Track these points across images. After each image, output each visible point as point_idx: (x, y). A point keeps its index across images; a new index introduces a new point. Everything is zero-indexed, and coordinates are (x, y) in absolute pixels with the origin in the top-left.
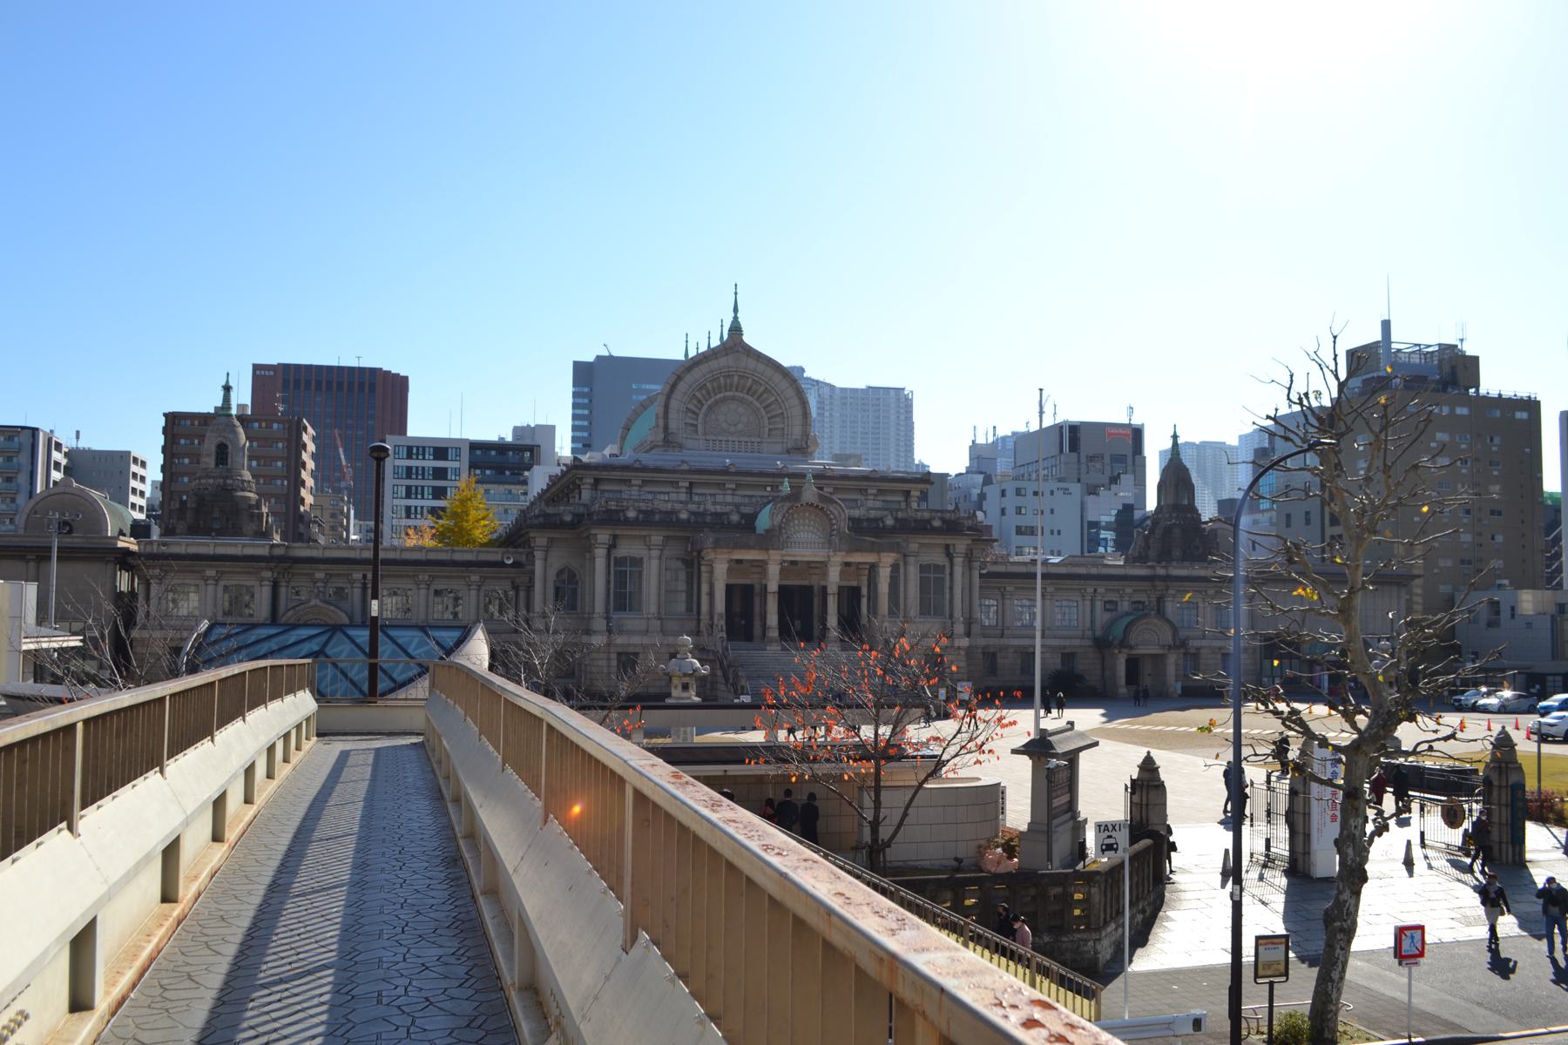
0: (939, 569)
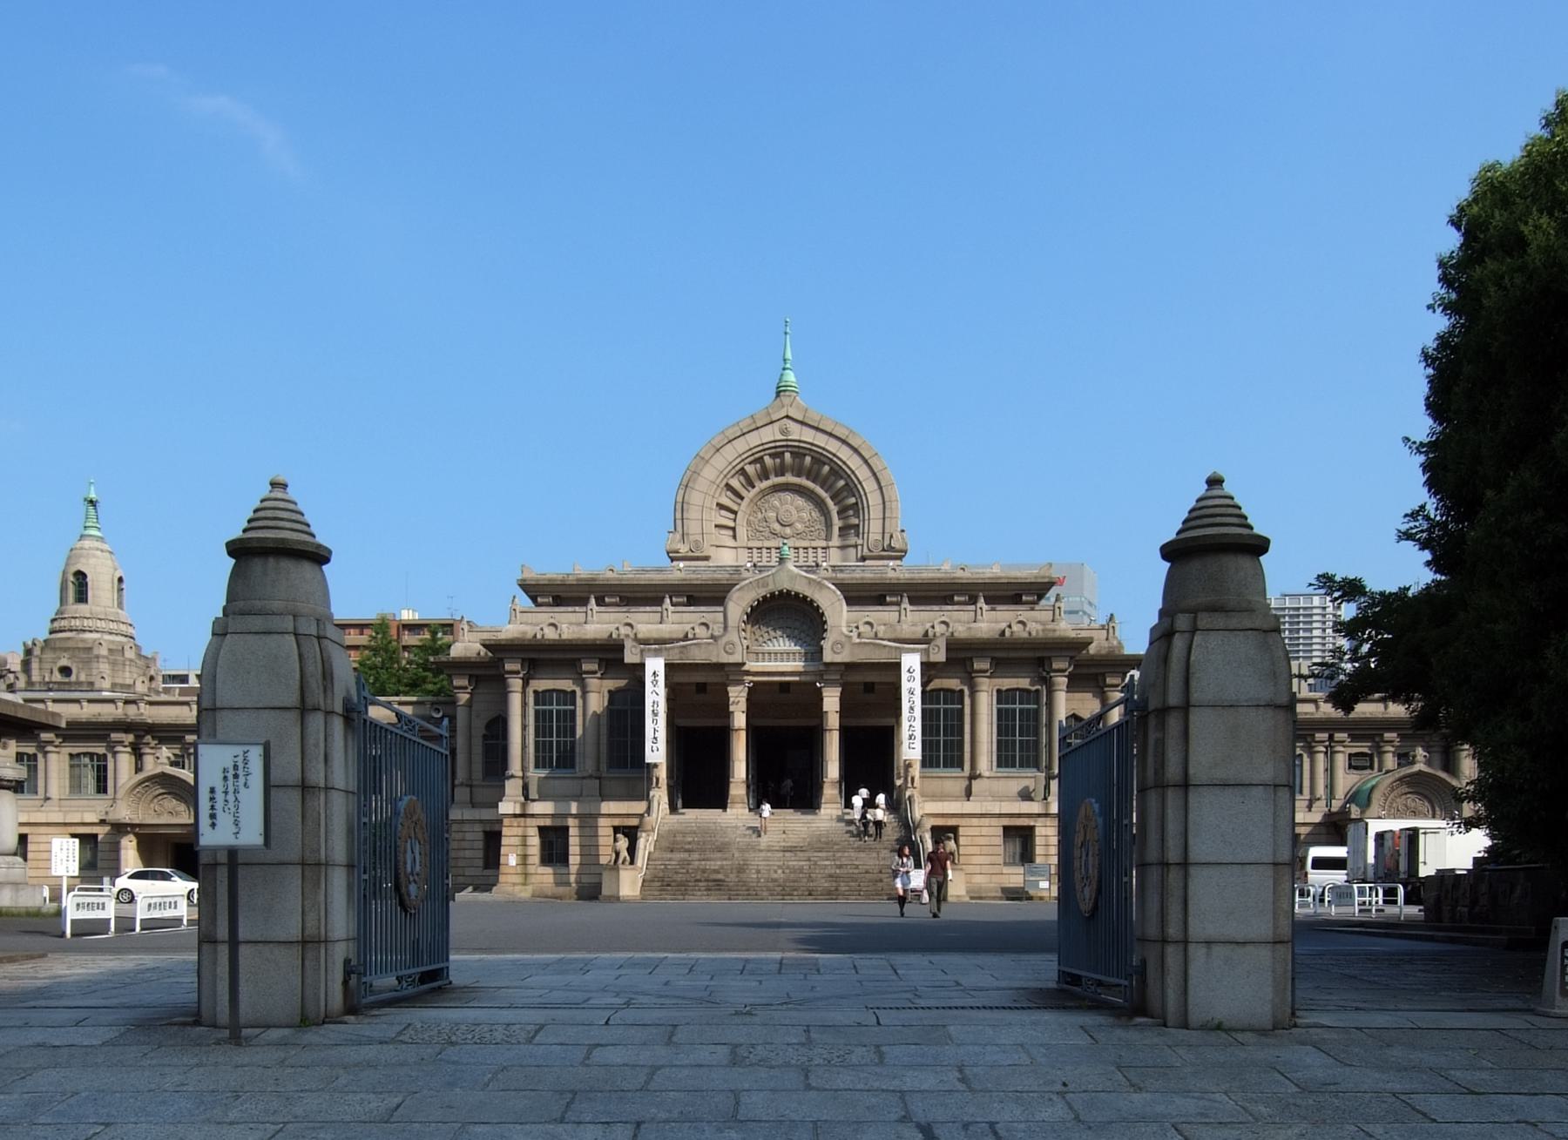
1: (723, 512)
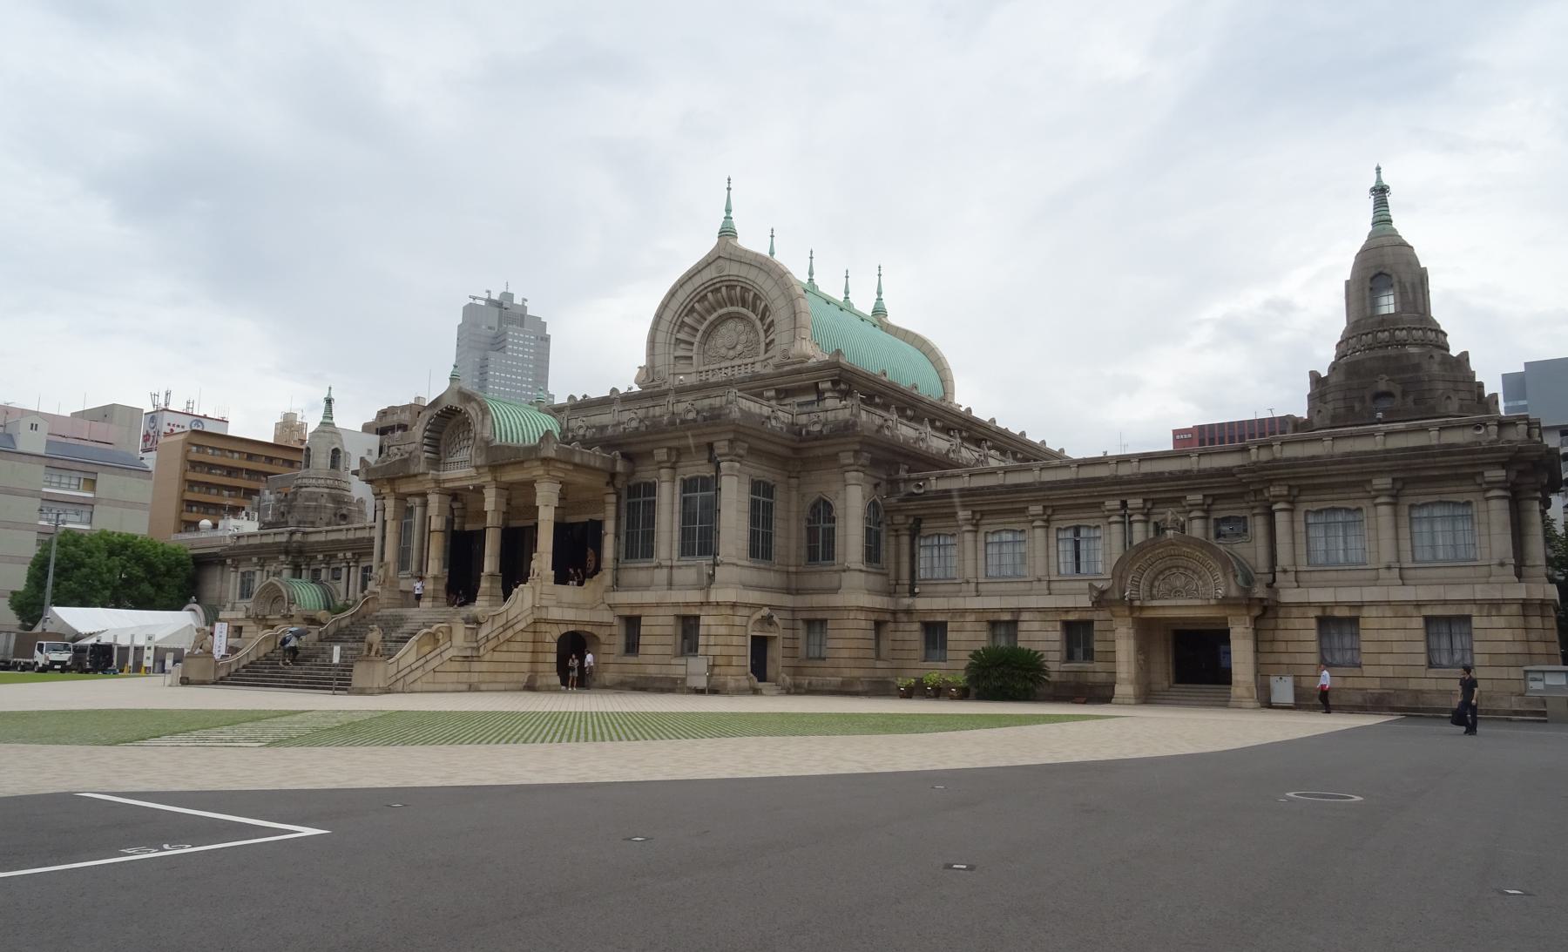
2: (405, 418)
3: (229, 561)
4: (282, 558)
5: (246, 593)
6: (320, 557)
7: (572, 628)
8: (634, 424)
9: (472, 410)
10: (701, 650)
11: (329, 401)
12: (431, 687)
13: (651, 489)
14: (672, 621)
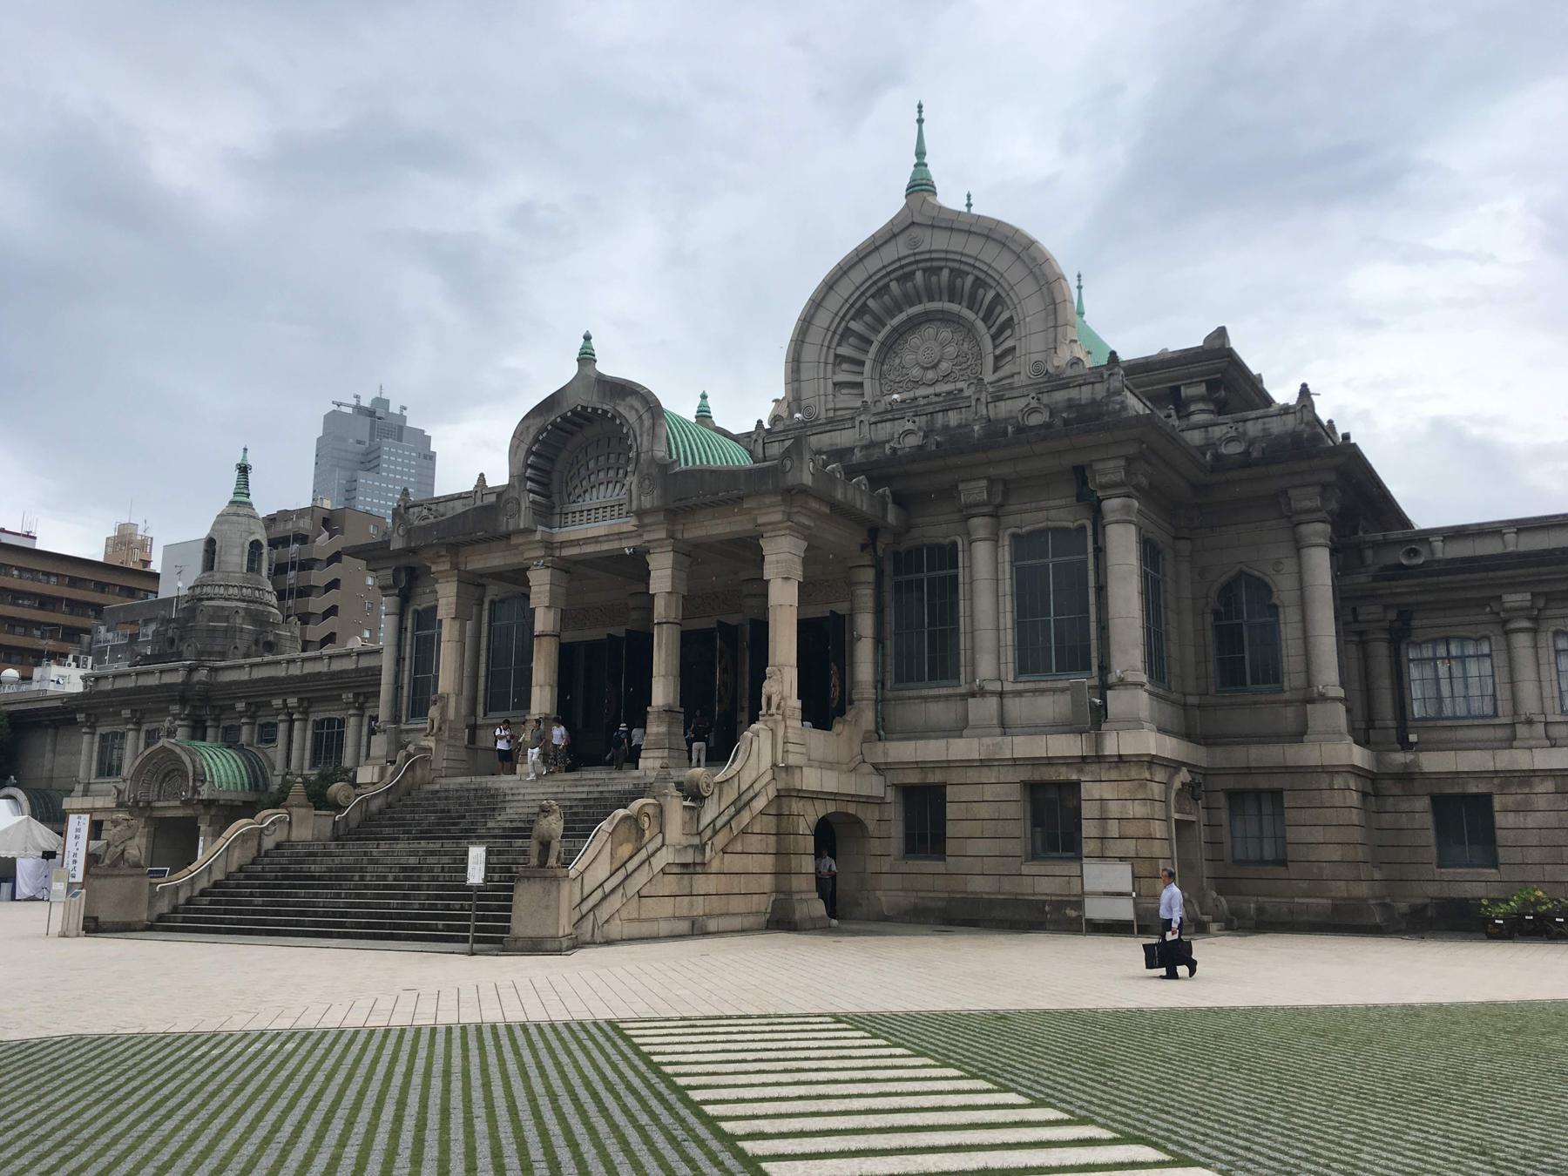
0: (1068, 538)
1: (845, 366)
2: (305, 525)
3: (81, 717)
4: (175, 709)
5: (107, 769)
6: (240, 706)
7: (831, 808)
8: (912, 441)
9: (628, 411)
10: (1088, 847)
11: (244, 470)
12: (646, 929)
13: (947, 556)
14: (1015, 792)
